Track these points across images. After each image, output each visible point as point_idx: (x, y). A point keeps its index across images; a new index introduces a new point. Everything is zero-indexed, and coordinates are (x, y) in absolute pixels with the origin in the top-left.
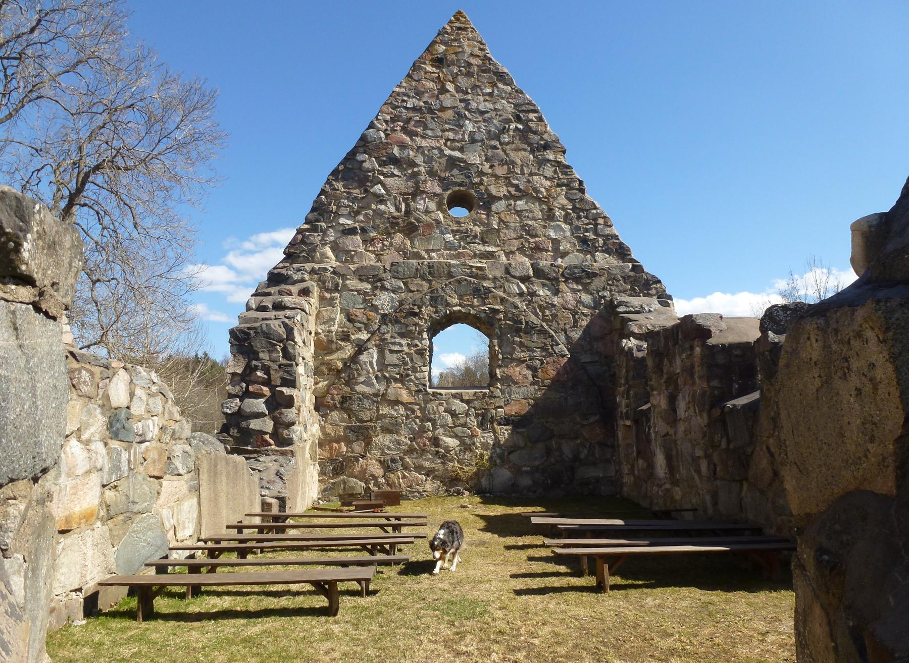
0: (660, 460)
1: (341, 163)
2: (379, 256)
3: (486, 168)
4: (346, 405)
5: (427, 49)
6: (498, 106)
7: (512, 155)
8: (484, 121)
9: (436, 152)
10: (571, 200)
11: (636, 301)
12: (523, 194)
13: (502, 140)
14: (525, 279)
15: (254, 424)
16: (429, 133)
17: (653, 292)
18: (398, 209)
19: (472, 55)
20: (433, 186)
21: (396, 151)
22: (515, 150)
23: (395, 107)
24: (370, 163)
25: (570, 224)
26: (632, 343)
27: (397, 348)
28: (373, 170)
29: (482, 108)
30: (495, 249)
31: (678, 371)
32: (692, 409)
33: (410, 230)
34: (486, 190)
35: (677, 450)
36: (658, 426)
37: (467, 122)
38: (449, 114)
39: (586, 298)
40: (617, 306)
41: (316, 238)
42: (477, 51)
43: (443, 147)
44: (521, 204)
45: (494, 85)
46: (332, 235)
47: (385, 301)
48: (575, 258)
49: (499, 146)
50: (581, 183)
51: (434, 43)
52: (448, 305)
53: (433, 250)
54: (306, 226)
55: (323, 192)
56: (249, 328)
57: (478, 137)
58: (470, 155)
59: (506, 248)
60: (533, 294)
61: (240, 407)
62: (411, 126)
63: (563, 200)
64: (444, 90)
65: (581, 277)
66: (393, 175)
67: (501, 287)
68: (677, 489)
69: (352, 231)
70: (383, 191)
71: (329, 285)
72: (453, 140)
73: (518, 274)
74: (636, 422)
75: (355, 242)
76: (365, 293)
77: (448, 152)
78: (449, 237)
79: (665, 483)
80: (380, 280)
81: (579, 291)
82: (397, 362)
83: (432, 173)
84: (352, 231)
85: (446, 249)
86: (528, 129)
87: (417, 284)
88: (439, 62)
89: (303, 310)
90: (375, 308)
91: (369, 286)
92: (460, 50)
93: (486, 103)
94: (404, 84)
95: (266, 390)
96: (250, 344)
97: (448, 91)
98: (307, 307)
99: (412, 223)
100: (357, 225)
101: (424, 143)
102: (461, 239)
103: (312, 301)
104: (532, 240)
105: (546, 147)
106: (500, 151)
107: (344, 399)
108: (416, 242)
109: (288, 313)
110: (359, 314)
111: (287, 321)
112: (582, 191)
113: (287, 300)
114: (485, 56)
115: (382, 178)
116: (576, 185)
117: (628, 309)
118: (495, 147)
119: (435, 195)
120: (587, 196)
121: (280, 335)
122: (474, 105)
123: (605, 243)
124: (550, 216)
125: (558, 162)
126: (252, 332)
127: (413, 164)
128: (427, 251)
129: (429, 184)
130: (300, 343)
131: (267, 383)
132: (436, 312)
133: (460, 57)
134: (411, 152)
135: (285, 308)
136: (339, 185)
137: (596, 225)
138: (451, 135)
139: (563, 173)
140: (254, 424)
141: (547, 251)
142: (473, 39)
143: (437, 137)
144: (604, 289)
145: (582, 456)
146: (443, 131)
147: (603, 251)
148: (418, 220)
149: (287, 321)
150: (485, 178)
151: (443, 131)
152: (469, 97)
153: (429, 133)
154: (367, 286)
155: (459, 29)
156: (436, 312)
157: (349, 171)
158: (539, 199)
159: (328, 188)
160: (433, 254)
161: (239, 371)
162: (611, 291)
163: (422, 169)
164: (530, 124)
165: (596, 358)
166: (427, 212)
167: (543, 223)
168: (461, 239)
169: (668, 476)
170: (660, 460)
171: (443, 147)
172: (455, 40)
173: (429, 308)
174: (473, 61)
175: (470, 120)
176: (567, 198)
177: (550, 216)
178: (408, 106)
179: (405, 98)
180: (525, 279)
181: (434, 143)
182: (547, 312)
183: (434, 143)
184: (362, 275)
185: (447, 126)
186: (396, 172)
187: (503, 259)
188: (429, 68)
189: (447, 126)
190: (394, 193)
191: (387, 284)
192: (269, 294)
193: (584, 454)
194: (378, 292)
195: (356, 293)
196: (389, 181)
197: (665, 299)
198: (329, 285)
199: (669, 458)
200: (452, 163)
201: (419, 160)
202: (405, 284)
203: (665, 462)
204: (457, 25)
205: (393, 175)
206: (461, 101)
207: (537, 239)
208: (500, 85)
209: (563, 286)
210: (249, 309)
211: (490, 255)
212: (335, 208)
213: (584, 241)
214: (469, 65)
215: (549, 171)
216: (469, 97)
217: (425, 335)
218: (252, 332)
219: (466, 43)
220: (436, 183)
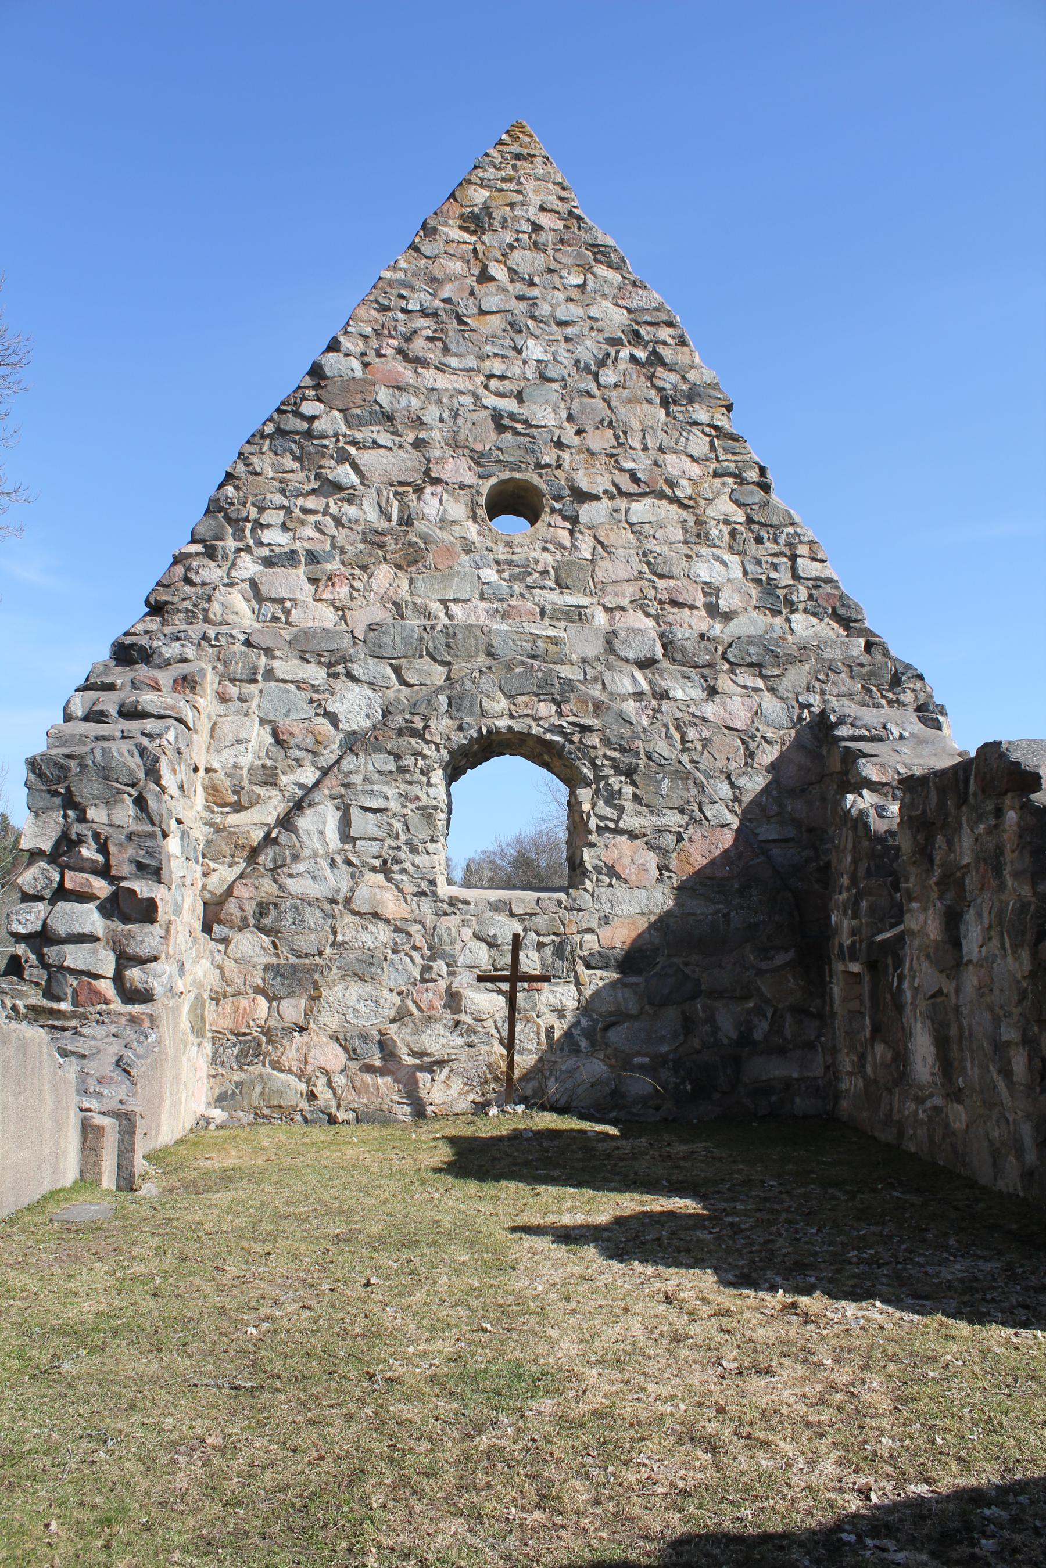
0: (922, 1047)
1: (270, 419)
2: (341, 610)
3: (569, 436)
4: (267, 921)
5: (452, 195)
6: (593, 312)
7: (622, 410)
8: (567, 340)
9: (467, 400)
10: (740, 504)
11: (871, 717)
12: (642, 488)
13: (602, 380)
14: (646, 664)
15: (75, 957)
16: (453, 361)
17: (908, 697)
19: (542, 209)
20: (457, 469)
21: (384, 396)
22: (630, 401)
23: (384, 309)
24: (330, 422)
25: (742, 553)
26: (867, 800)
27: (374, 804)
28: (336, 435)
29: (562, 315)
31: (966, 860)
32: (996, 941)
33: (411, 559)
34: (570, 480)
35: (961, 1027)
36: (920, 975)
37: (531, 342)
38: (495, 323)
39: (770, 704)
40: (834, 726)
41: (211, 573)
42: (553, 202)
43: (481, 391)
44: (641, 509)
45: (588, 269)
46: (248, 567)
47: (355, 706)
48: (752, 623)
49: (595, 391)
50: (763, 471)
52: (484, 714)
53: (455, 601)
54: (198, 548)
55: (229, 477)
56: (68, 756)
57: (550, 374)
58: (534, 408)
60: (663, 695)
61: (45, 924)
62: (419, 346)
63: (724, 506)
64: (485, 277)
65: (765, 661)
66: (376, 445)
67: (595, 679)
68: (960, 1107)
69: (291, 558)
70: (354, 479)
71: (238, 669)
72: (502, 378)
73: (631, 655)
74: (872, 966)
75: (292, 582)
76: (315, 689)
77: (490, 401)
78: (490, 574)
79: (931, 1095)
80: (345, 660)
81: (757, 690)
82: (376, 832)
83: (455, 444)
84: (291, 558)
85: (483, 598)
86: (656, 359)
87: (420, 672)
88: (476, 222)
89: (180, 720)
90: (333, 719)
91: (323, 672)
92: (520, 198)
93: (571, 306)
94: (402, 264)
95: (101, 887)
96: (68, 789)
97: (492, 279)
98: (189, 716)
99: (411, 544)
100: (298, 546)
101: (442, 382)
102: (513, 578)
103: (201, 702)
104: (661, 583)
105: (693, 396)
106: (598, 403)
107: (262, 909)
108: (419, 583)
109: (150, 725)
110: (298, 729)
111: (145, 741)
112: (765, 487)
113: (148, 700)
114: (570, 213)
115: (352, 450)
116: (753, 475)
117: (857, 732)
119: (462, 487)
120: (774, 497)
121: (131, 773)
122: (544, 309)
123: (811, 597)
124: (699, 534)
125: (716, 428)
126: (73, 764)
127: (419, 422)
128: (444, 602)
129: (450, 465)
130: (173, 789)
131: (104, 872)
132: (460, 728)
133: (518, 212)
134: (414, 401)
135: (144, 715)
136: (264, 464)
137: (793, 558)
138: (497, 367)
140: (75, 957)
141: (692, 607)
143: (470, 370)
145: (758, 1035)
146: (482, 358)
148: (426, 538)
149: (145, 741)
150: (566, 456)
151: (482, 358)
152: (535, 292)
153: (453, 361)
154: (316, 674)
155: (518, 157)
156: (460, 728)
157: (286, 430)
158: (674, 500)
159: (241, 468)
160: (454, 608)
161: (47, 846)
162: (823, 693)
163: (436, 435)
164: (660, 349)
165: (790, 832)
166: (444, 523)
167: (685, 550)
168: (513, 578)
169: (938, 1080)
170: (922, 1047)
171: (481, 391)
173: (446, 721)
174: (546, 221)
175: (537, 337)
176: (737, 502)
177: (699, 534)
178: (410, 307)
179: (405, 292)
180: (646, 664)
181: (461, 383)
182: (692, 734)
183: (461, 383)
184: (305, 647)
185: (489, 349)
186: (384, 439)
187: (601, 619)
188: (456, 234)
189: (489, 349)
190: (376, 479)
191: (357, 670)
192: (111, 687)
193: (761, 1029)
194: (337, 685)
195: (291, 687)
196: (366, 458)
197: (929, 714)
198: (238, 669)
199: (942, 1043)
200: (500, 422)
201: (432, 414)
202: (397, 670)
203: (933, 1049)
204: (515, 149)
205: (376, 445)
206: (521, 298)
207: (672, 582)
208: (602, 271)
209: (724, 682)
210: (68, 718)
211: (577, 616)
212: (254, 513)
213: (769, 587)
214: (537, 228)
215: (699, 444)
216: (535, 292)
217: (438, 777)
218: (73, 764)
219: (530, 185)
220: (464, 462)
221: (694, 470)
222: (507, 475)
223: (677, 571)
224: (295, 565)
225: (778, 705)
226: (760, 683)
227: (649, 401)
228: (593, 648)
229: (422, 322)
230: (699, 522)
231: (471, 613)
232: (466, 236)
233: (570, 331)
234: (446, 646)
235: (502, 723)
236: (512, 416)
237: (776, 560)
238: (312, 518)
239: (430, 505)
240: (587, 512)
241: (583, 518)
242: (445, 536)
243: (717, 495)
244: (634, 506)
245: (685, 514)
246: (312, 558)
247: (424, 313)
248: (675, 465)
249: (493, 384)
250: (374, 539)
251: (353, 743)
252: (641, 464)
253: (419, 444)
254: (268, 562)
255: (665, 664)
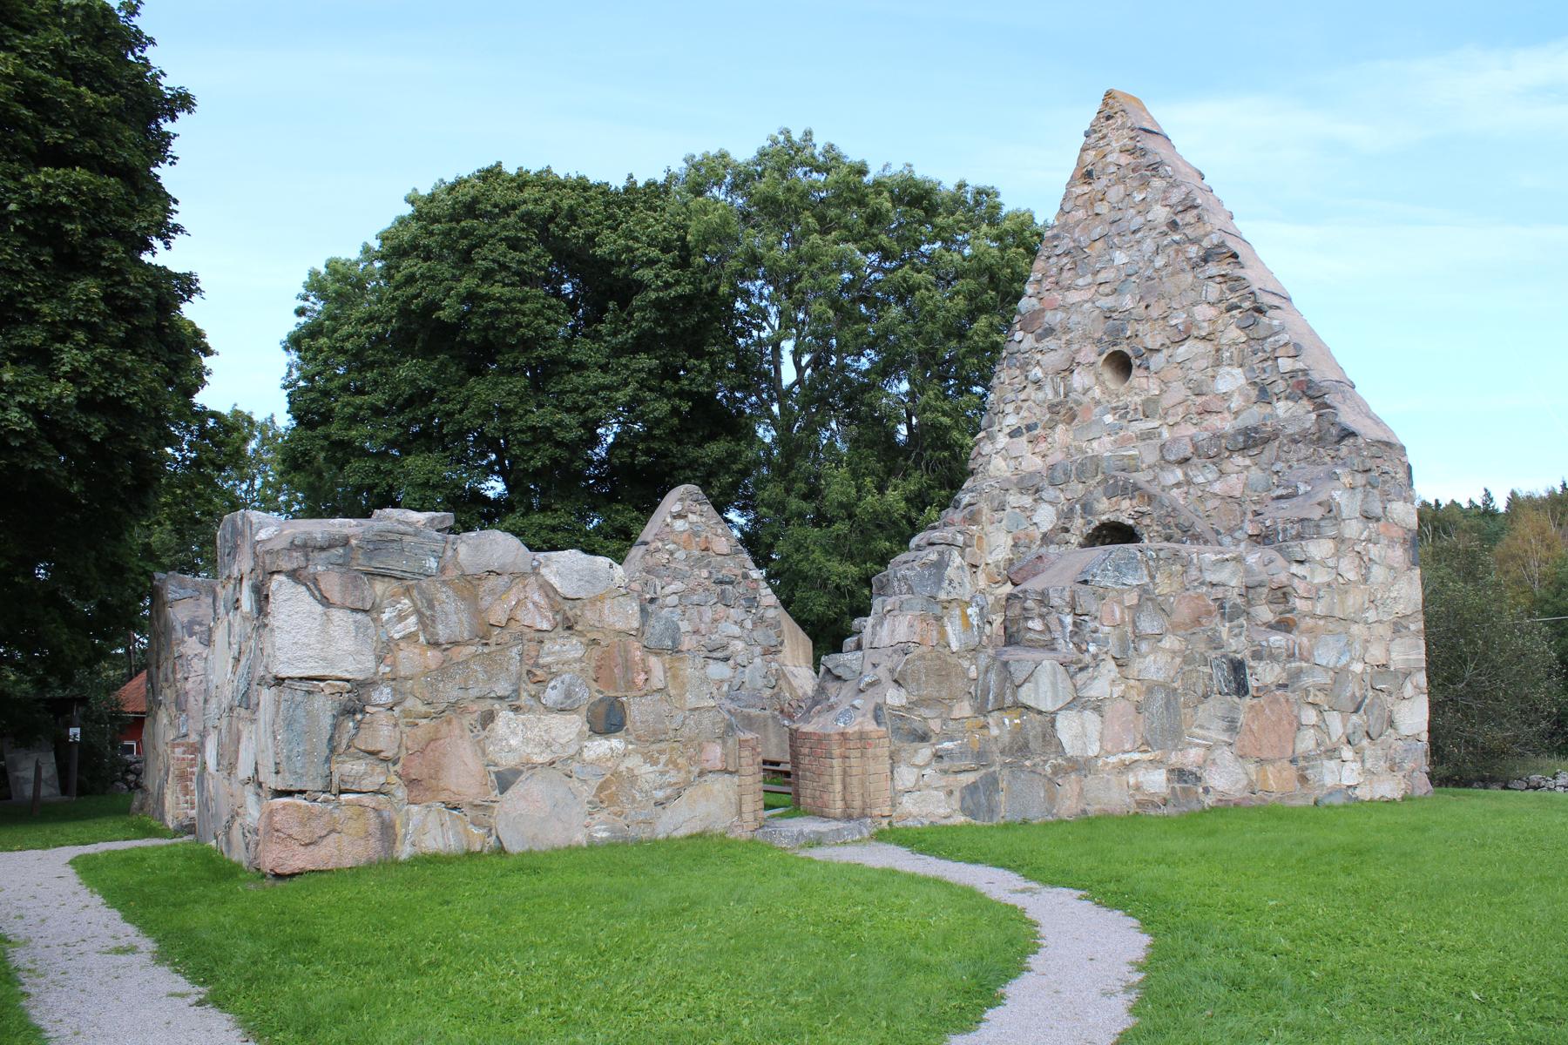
16: (1081, 282)
18: (1057, 393)
22: (1173, 274)
30: (1156, 424)
39: (1255, 473)
47: (1046, 517)
51: (1083, 150)
59: (1171, 421)
63: (1234, 333)
73: (1172, 458)
78: (1109, 419)
81: (1247, 467)
104: (1199, 400)
118: (1150, 278)
133: (1109, 159)
138: (1102, 277)
139: (1232, 290)
142: (1123, 126)
144: (1278, 458)
147: (1287, 398)
154: (1027, 501)
172: (1104, 137)
189: (1098, 266)
215: (1213, 290)
221: (1211, 312)
222: (1111, 350)
223: (1205, 389)
224: (1021, 434)
225: (1260, 473)
226: (1248, 462)
227: (1183, 270)
228: (1151, 457)
229: (1065, 260)
230: (1218, 351)
231: (1102, 447)
232: (1086, 188)
233: (1139, 235)
234: (1087, 467)
235: (1104, 518)
236: (1111, 310)
237: (1265, 365)
238: (1026, 405)
239: (1079, 380)
240: (1156, 361)
241: (1152, 368)
242: (1086, 399)
243: (1226, 326)
244: (1182, 349)
245: (1209, 346)
246: (1029, 428)
247: (1067, 253)
248: (1203, 312)
249: (1102, 288)
250: (1053, 408)
251: (1046, 539)
252: (1179, 319)
253: (1069, 343)
254: (1012, 435)
255: (1195, 460)
